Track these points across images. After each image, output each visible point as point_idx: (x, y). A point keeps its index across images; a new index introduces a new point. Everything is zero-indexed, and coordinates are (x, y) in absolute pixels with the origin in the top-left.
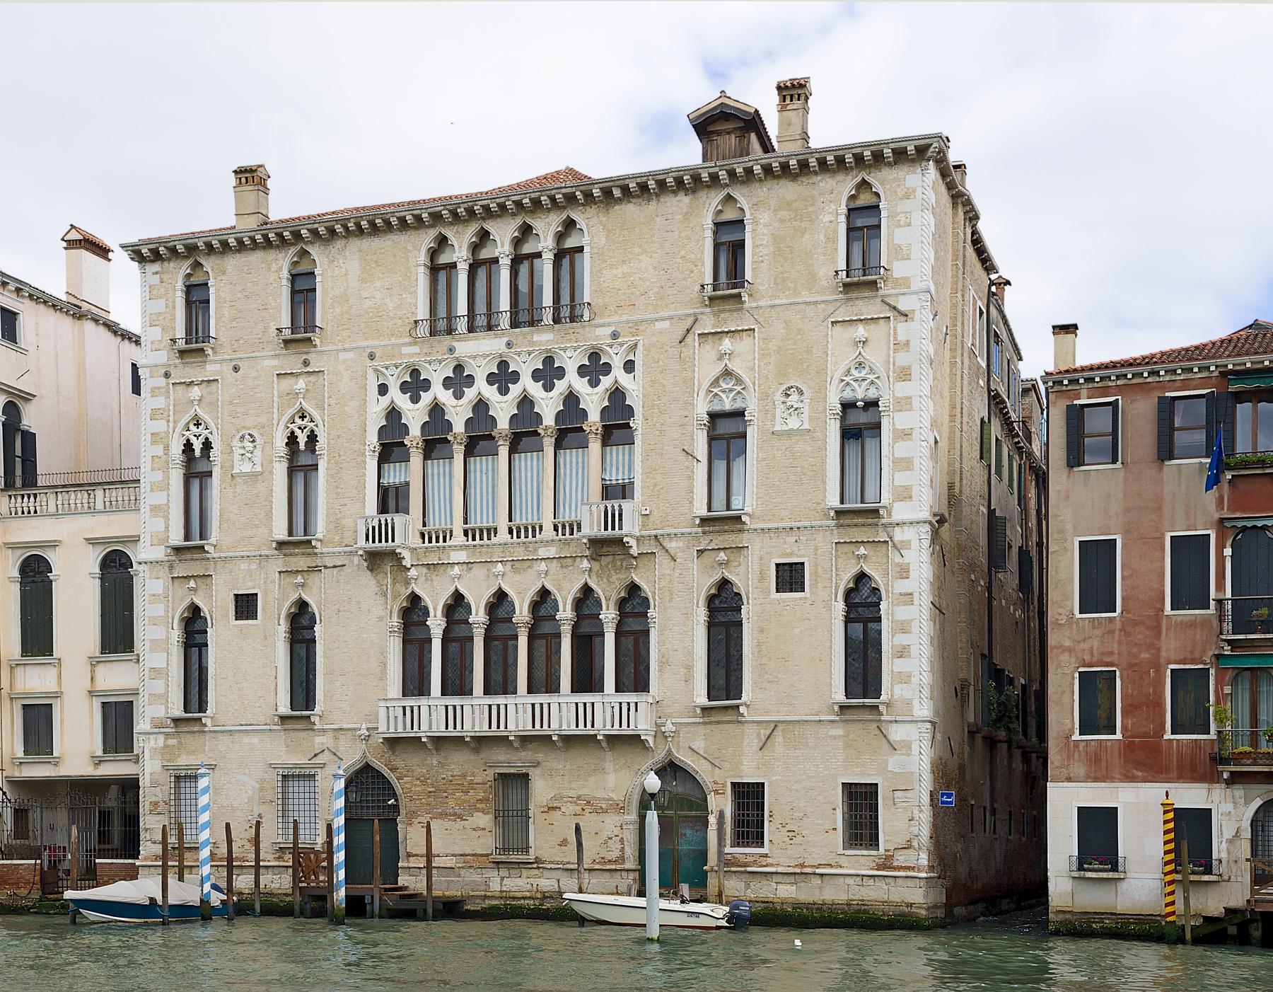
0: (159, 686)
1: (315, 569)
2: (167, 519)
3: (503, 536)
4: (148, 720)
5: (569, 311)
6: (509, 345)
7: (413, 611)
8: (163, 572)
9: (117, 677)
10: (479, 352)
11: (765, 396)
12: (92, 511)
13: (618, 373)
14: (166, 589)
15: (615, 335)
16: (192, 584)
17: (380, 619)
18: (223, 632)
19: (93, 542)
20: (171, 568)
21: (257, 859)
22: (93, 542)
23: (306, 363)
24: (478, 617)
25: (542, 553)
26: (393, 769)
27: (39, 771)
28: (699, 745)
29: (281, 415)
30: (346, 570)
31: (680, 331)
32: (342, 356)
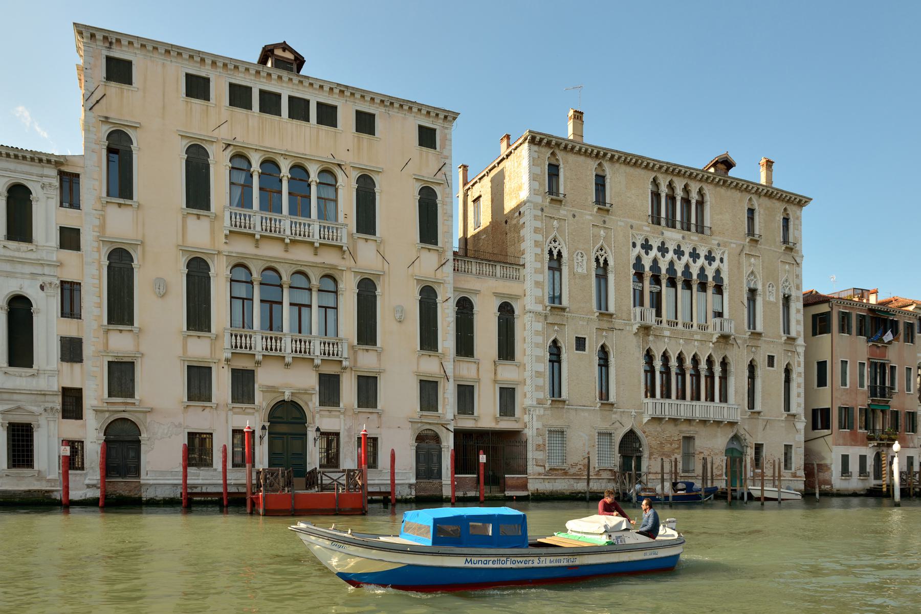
0: (540, 381)
1: (612, 329)
2: (543, 290)
3: (680, 326)
4: (535, 400)
5: (700, 229)
6: (683, 238)
7: (649, 357)
8: (542, 319)
9: (508, 373)
10: (673, 237)
11: (764, 285)
12: (494, 275)
13: (717, 261)
14: (543, 328)
15: (719, 245)
16: (556, 328)
17: (638, 359)
18: (568, 353)
19: (496, 295)
20: (546, 317)
21: (588, 475)
22: (496, 295)
23: (604, 222)
24: (688, 363)
25: (696, 337)
26: (644, 432)
27: (467, 423)
28: (746, 427)
29: (594, 247)
30: (624, 332)
31: (739, 250)
32: (619, 223)
